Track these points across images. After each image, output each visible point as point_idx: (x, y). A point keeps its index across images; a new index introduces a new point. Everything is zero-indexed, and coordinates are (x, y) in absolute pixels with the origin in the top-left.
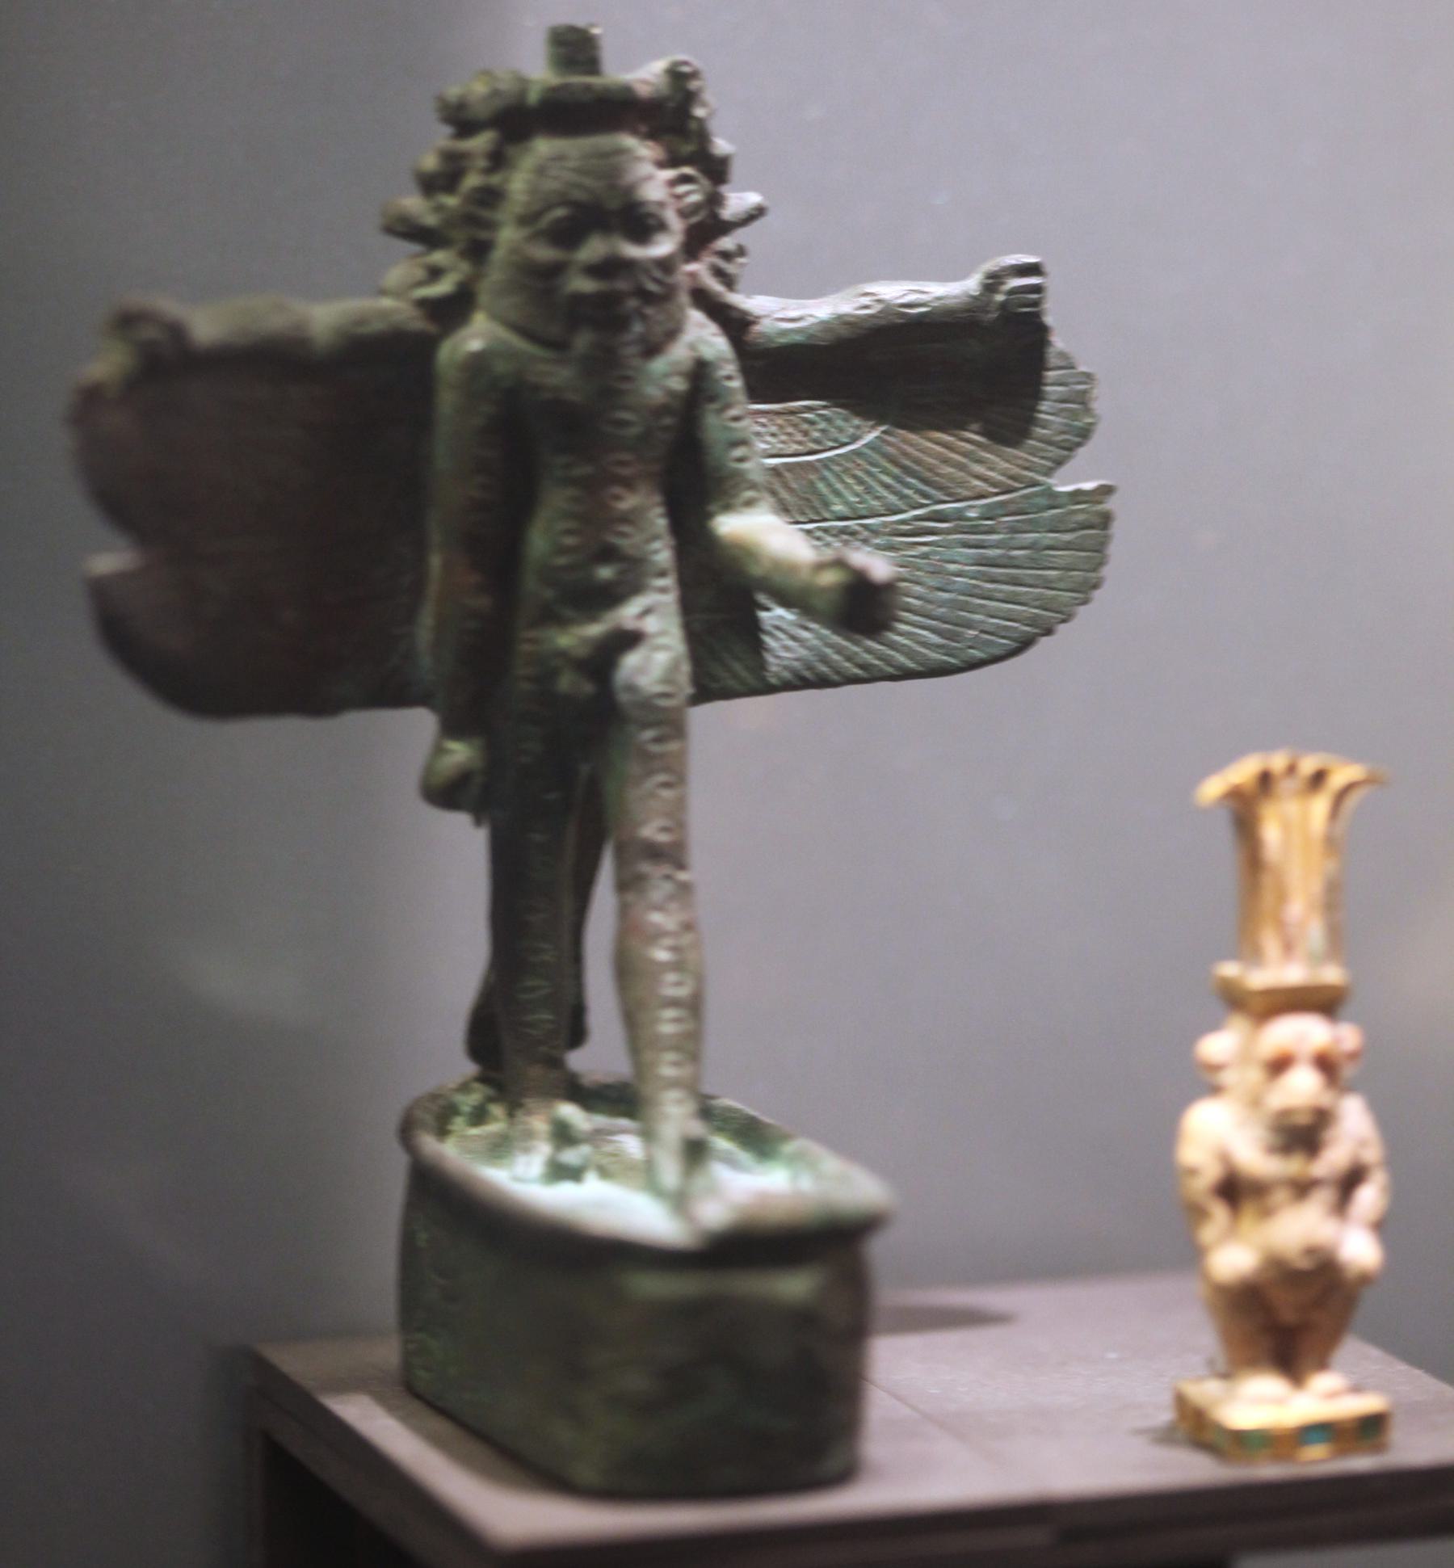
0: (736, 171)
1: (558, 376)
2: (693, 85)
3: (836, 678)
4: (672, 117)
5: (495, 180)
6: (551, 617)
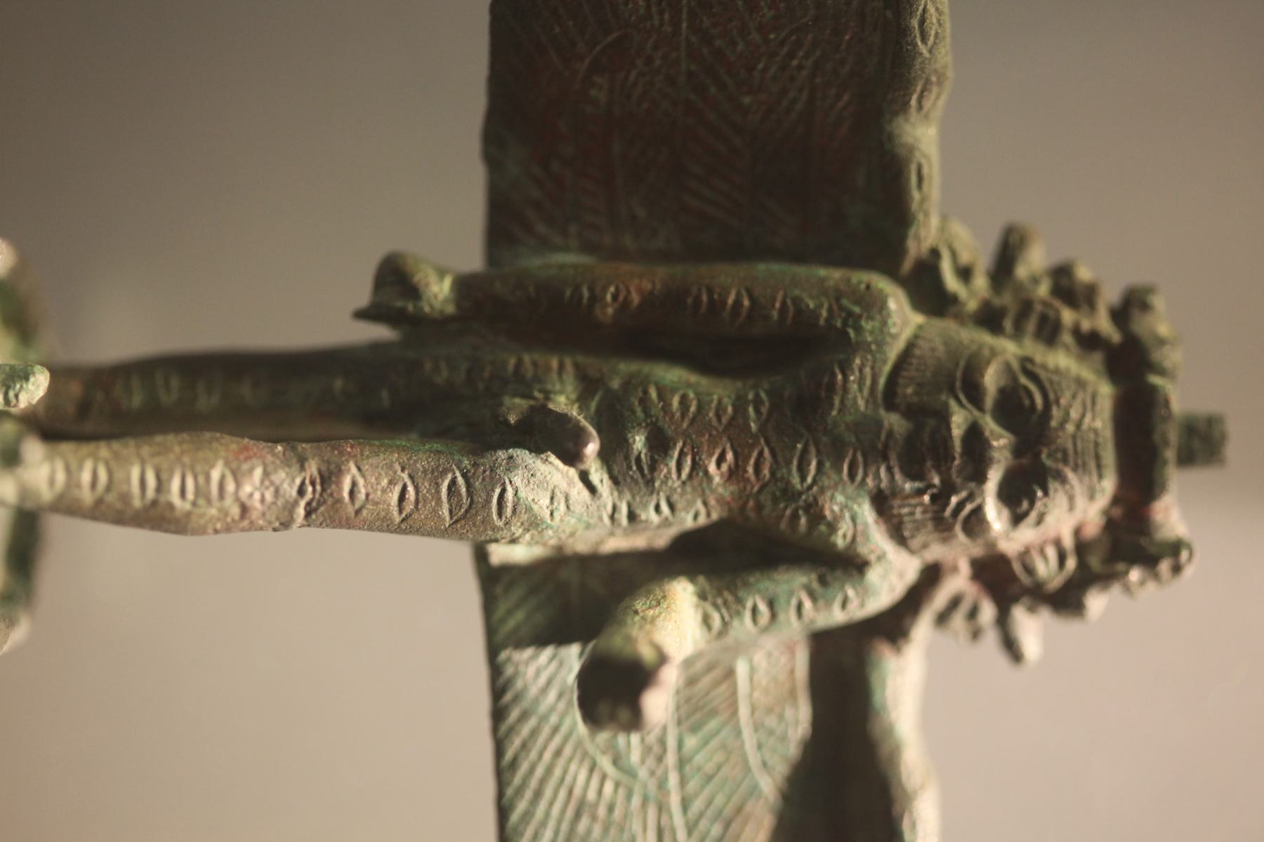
1: (858, 389)
2: (1164, 566)
3: (503, 728)
4: (1131, 543)
5: (1067, 338)
6: (588, 386)
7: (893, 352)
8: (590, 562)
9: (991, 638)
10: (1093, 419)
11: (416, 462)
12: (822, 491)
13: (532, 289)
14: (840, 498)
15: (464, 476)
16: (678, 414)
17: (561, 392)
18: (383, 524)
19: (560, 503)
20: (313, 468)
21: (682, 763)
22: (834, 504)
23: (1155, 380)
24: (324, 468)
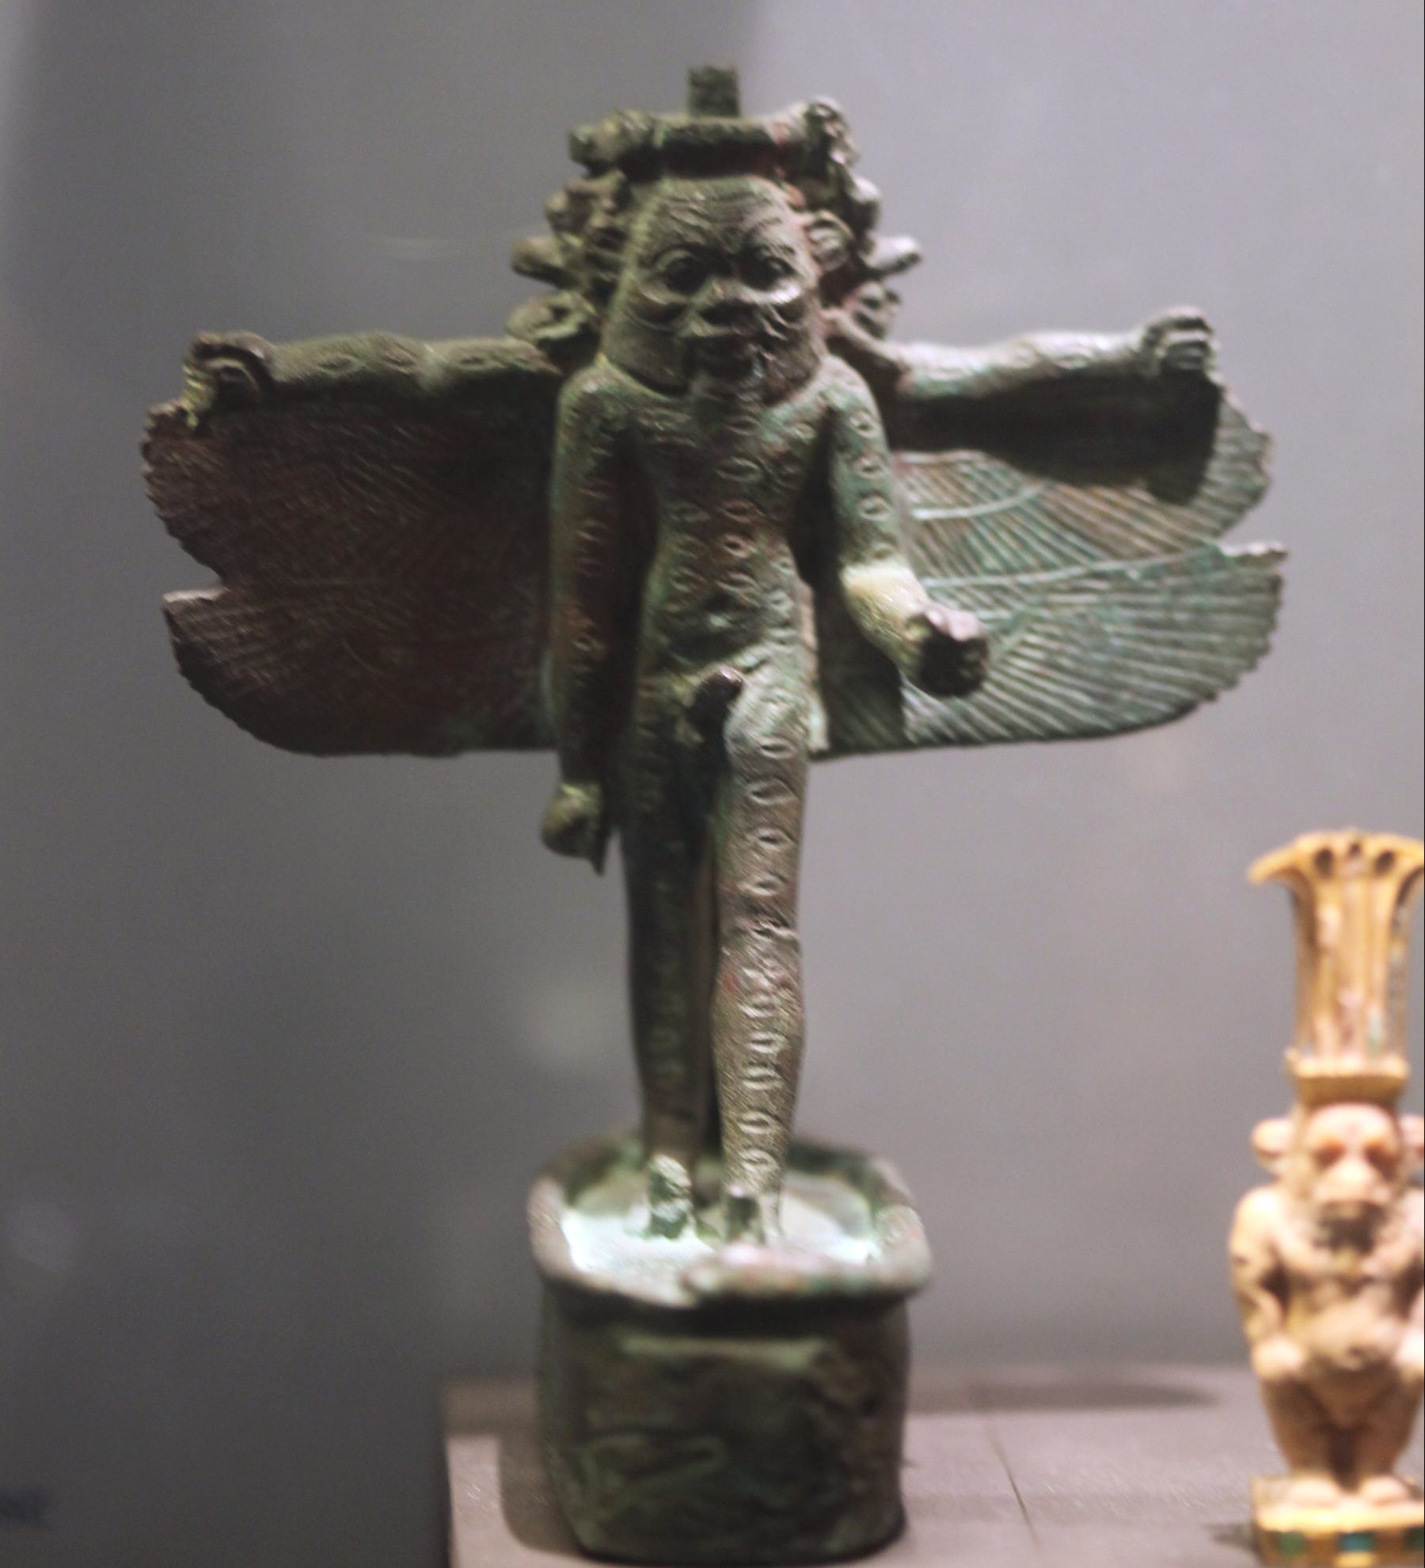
0: (886, 217)
1: (669, 420)
2: (830, 130)
4: (809, 161)
5: (619, 221)
6: (666, 664)
7: (635, 387)
8: (824, 656)
9: (894, 283)
10: (695, 201)
12: (764, 454)
18: (792, 858)
19: (773, 692)
20: (744, 923)
21: (1010, 570)
22: (774, 441)
23: (659, 139)
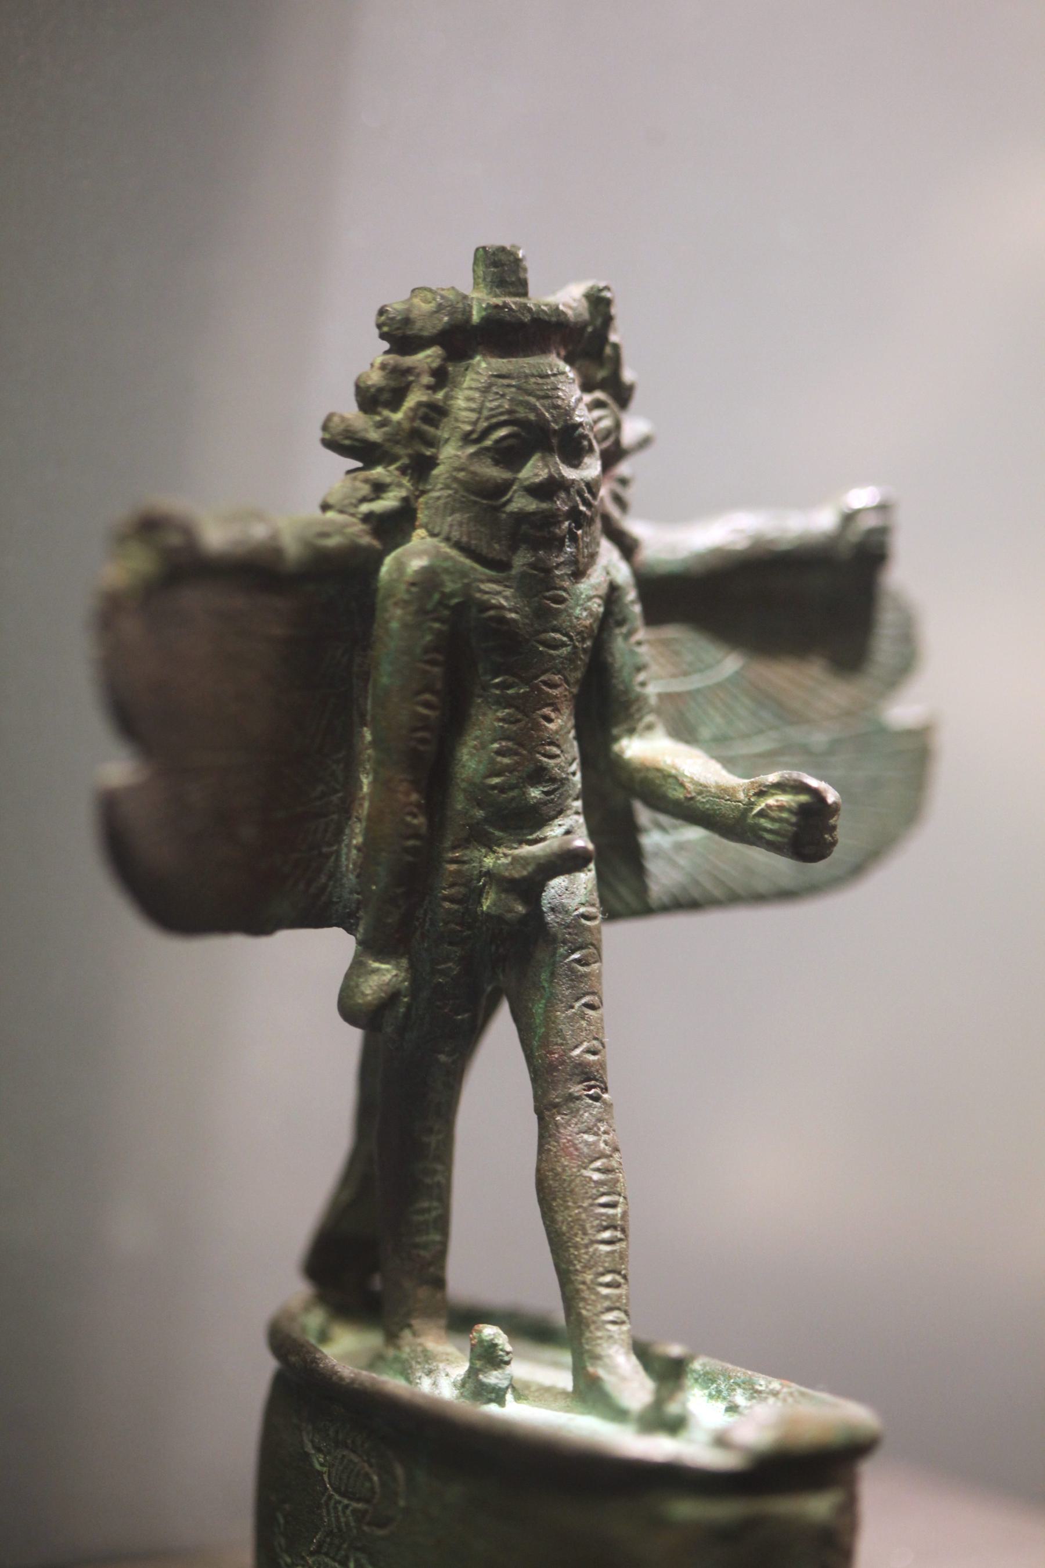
0: (637, 401)
4: (589, 341)
6: (480, 837)
11: (563, 996)
12: (573, 627)
13: (399, 891)
14: (578, 611)
15: (573, 952)
16: (516, 758)
17: (481, 861)
24: (578, 1079)
